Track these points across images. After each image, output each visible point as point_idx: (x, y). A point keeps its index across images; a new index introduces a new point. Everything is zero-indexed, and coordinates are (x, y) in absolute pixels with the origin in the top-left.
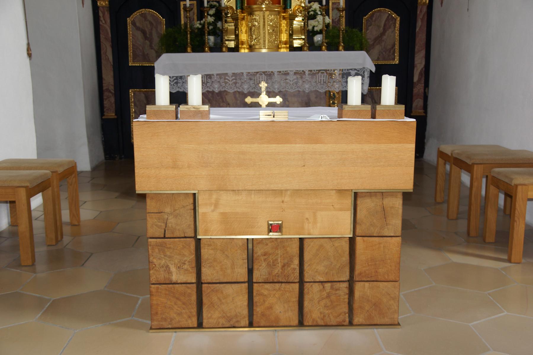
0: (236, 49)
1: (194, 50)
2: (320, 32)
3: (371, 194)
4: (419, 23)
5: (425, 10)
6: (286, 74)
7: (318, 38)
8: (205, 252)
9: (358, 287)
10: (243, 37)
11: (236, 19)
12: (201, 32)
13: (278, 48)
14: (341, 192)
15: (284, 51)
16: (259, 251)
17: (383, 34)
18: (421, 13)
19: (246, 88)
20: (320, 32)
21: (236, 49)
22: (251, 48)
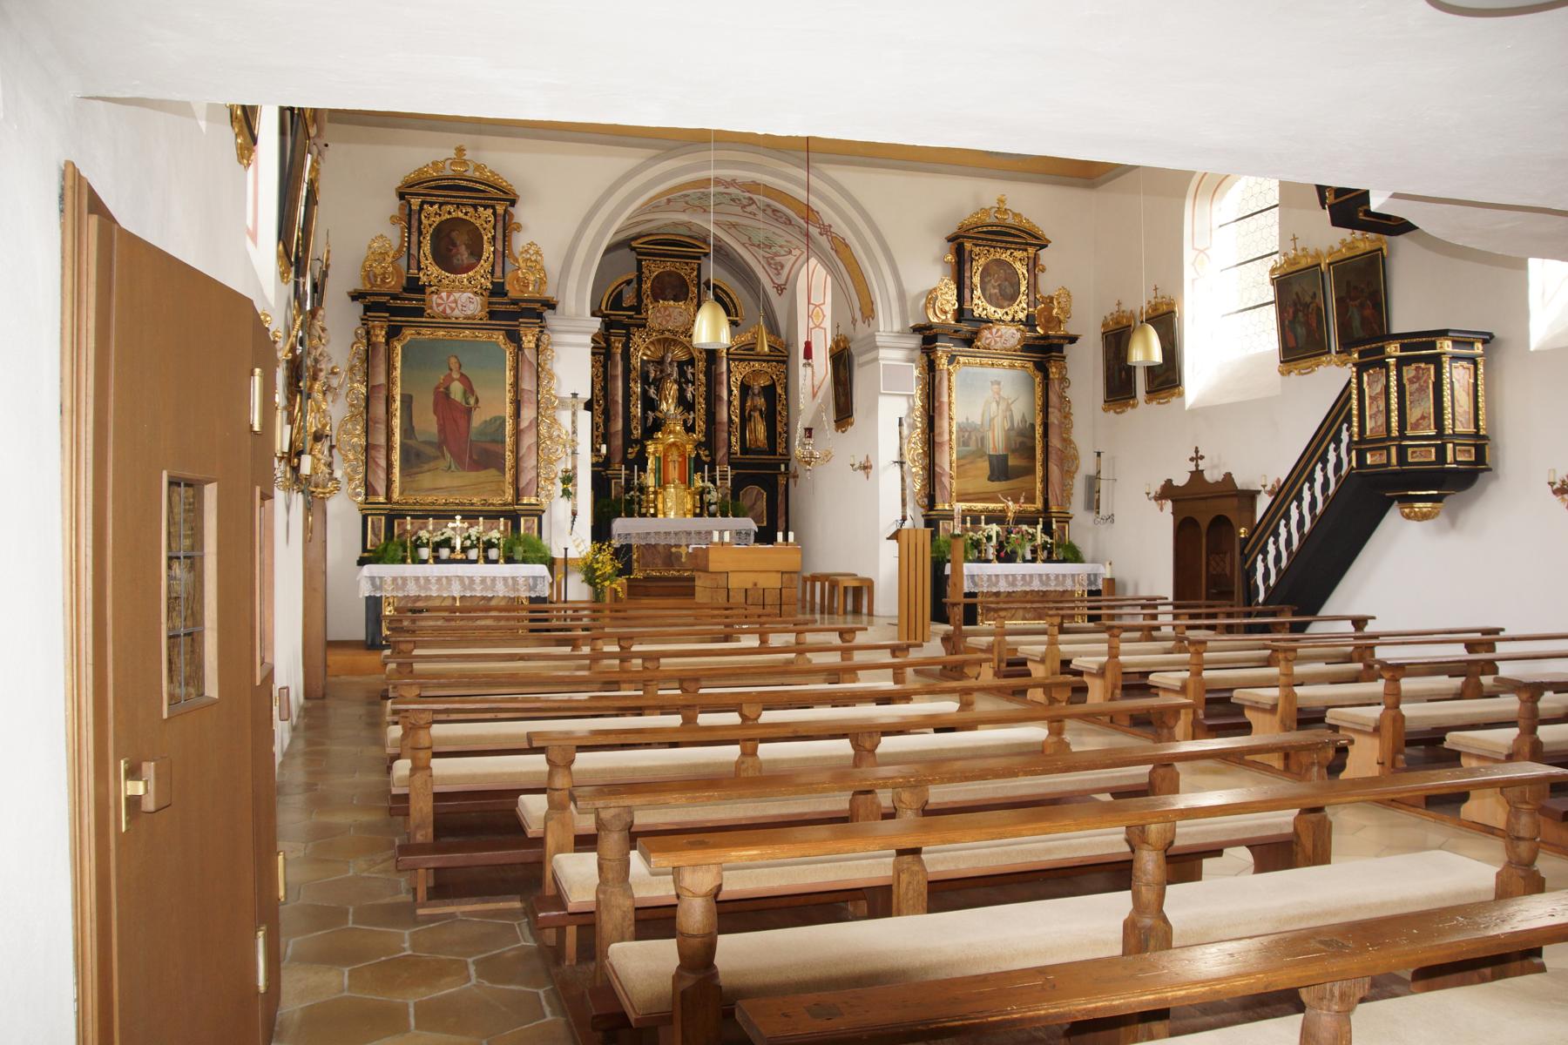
0: (654, 515)
1: (627, 516)
2: (715, 503)
3: (786, 572)
4: (780, 497)
5: (783, 488)
6: (700, 533)
7: (713, 508)
8: (731, 593)
9: (784, 607)
10: (660, 506)
11: (655, 493)
12: (630, 502)
13: (685, 514)
14: (778, 571)
15: (688, 516)
16: (749, 593)
17: (754, 504)
18: (781, 490)
19: (673, 542)
20: (715, 503)
21: (654, 515)
22: (664, 514)
